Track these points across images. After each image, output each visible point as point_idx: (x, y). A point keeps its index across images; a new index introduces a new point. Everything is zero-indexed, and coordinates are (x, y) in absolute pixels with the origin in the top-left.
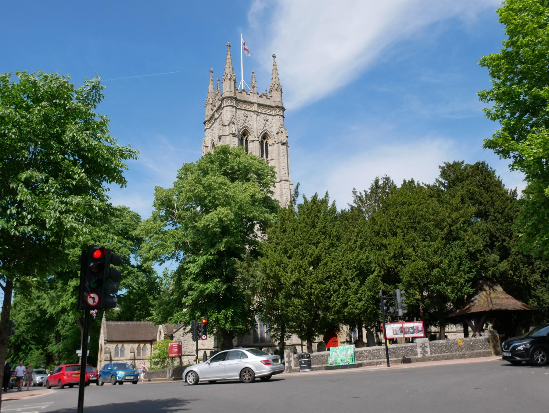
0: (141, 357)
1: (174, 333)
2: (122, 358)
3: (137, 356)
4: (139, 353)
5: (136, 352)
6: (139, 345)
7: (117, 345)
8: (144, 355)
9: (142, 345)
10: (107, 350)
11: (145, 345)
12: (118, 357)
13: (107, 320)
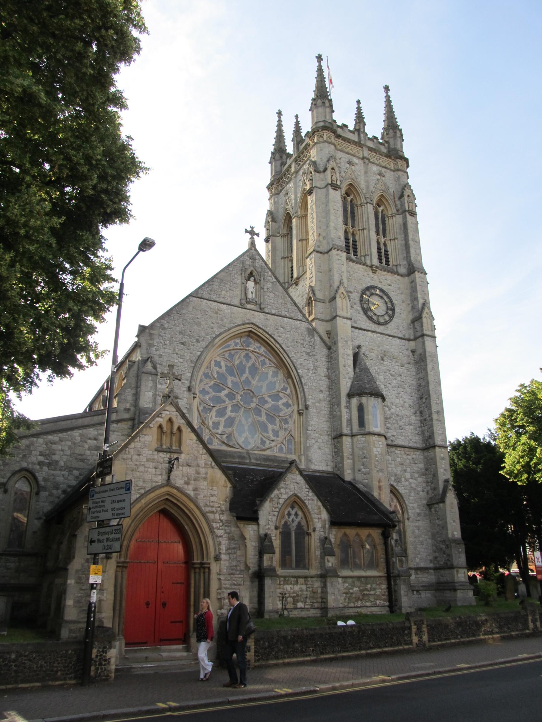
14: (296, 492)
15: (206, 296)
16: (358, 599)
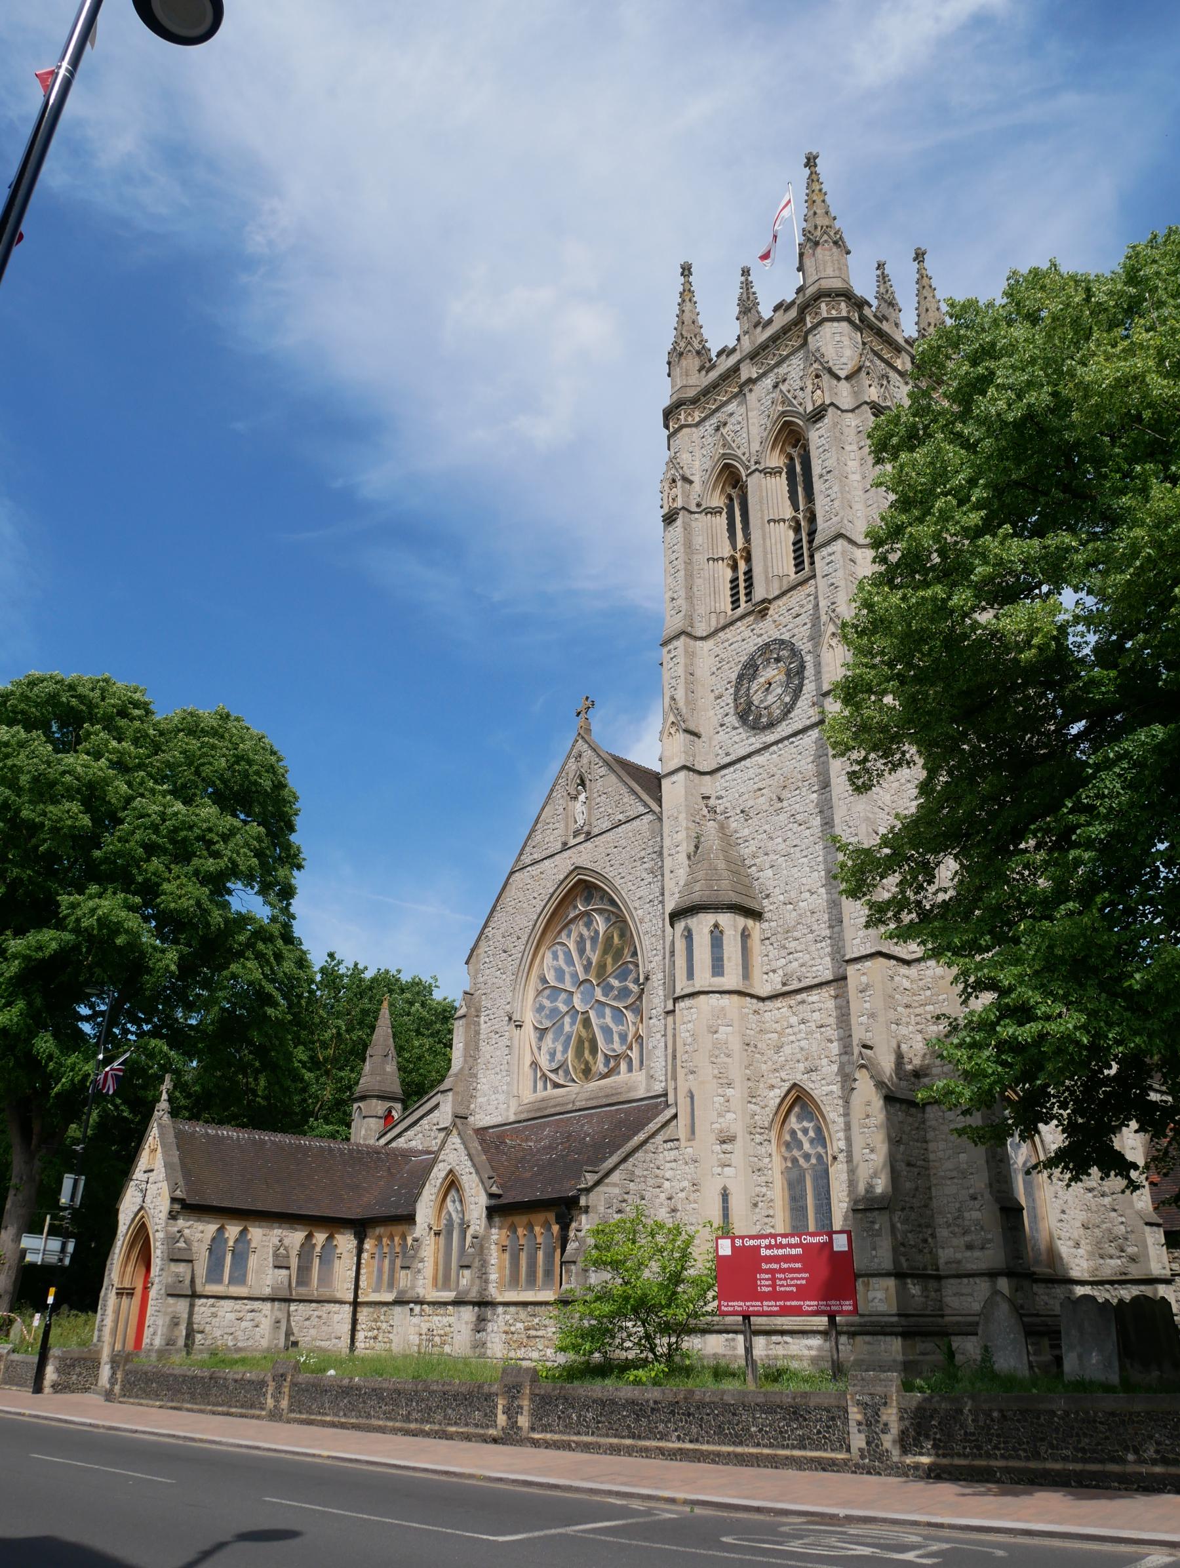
0: (314, 1287)
1: (588, 1190)
2: (235, 1290)
3: (299, 1283)
4: (304, 1270)
5: (294, 1262)
6: (309, 1236)
8: (326, 1277)
9: (320, 1238)
10: (181, 1245)
11: (330, 1238)
12: (219, 1281)
13: (174, 1113)
15: (528, 861)
16: (521, 1345)
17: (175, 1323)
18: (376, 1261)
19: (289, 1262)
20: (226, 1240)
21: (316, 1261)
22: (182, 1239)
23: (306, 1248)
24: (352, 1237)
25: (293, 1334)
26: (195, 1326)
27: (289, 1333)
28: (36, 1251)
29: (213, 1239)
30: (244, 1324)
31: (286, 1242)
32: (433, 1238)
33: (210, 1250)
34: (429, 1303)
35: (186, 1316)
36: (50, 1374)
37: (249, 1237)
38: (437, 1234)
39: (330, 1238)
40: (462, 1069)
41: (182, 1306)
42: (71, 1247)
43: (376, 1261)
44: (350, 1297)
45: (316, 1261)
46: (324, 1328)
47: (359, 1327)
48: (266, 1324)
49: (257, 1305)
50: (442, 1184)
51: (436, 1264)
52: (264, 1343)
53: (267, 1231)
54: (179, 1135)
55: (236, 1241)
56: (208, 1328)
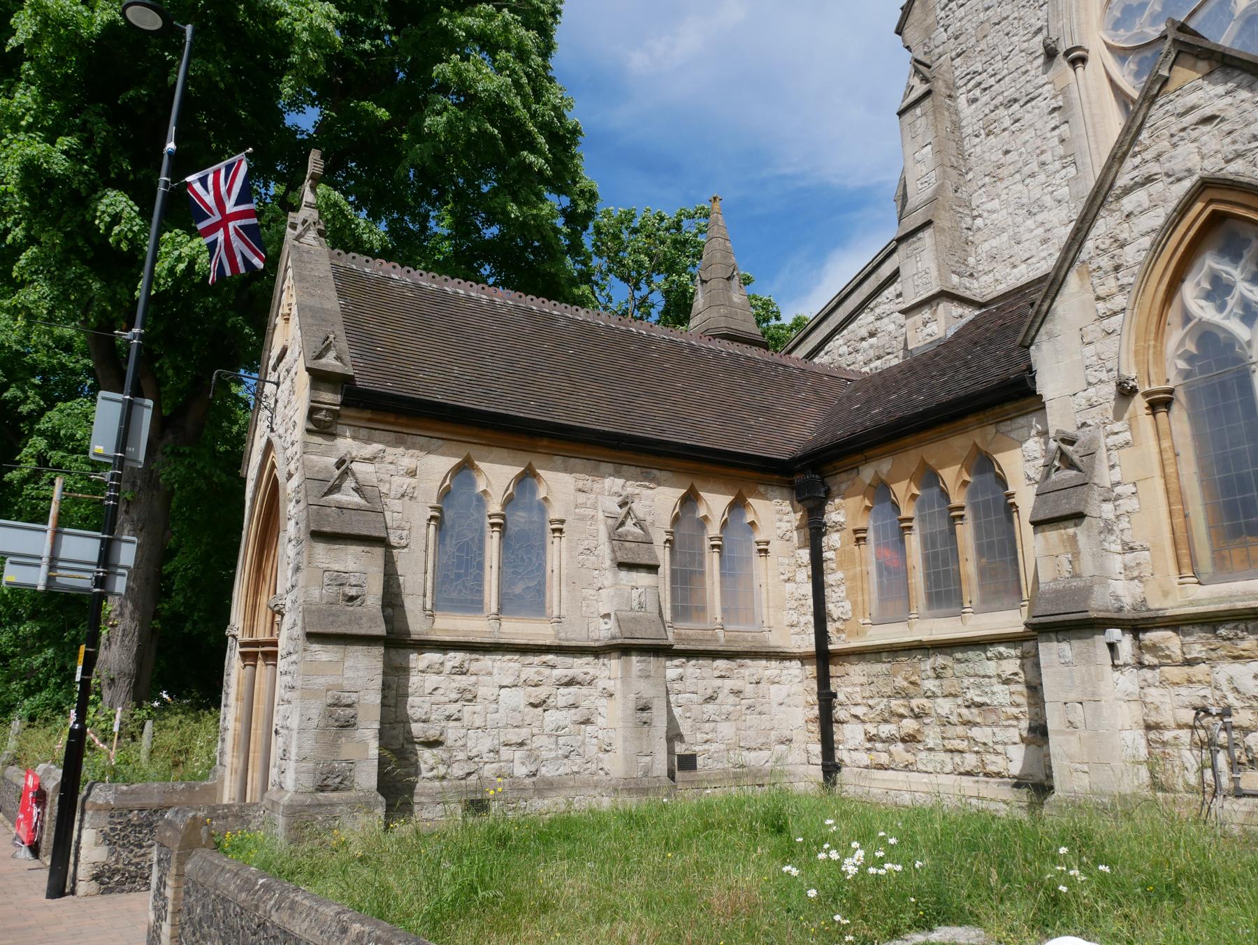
0: (712, 624)
2: (517, 629)
4: (686, 579)
6: (690, 500)
7: (465, 468)
9: (715, 503)
11: (738, 505)
12: (474, 605)
14: (1212, 166)
17: (340, 720)
18: (869, 551)
19: (652, 553)
20: (482, 498)
21: (712, 561)
22: (349, 483)
23: (685, 529)
24: (786, 506)
25: (680, 737)
26: (416, 728)
27: (674, 736)
28: (29, 560)
29: (445, 494)
30: (552, 718)
31: (638, 508)
32: (1146, 421)
33: (438, 520)
34: (1177, 624)
35: (372, 698)
36: (91, 849)
37: (542, 493)
38: (1160, 403)
39: (738, 505)
40: (940, 189)
41: (361, 671)
42: (127, 554)
43: (869, 551)
44: (808, 643)
45: (712, 561)
46: (752, 719)
47: (839, 713)
48: (613, 717)
49: (579, 666)
50: (1157, 249)
51: (1174, 495)
52: (615, 765)
53: (585, 480)
54: (346, 283)
55: (508, 501)
56: (452, 733)
